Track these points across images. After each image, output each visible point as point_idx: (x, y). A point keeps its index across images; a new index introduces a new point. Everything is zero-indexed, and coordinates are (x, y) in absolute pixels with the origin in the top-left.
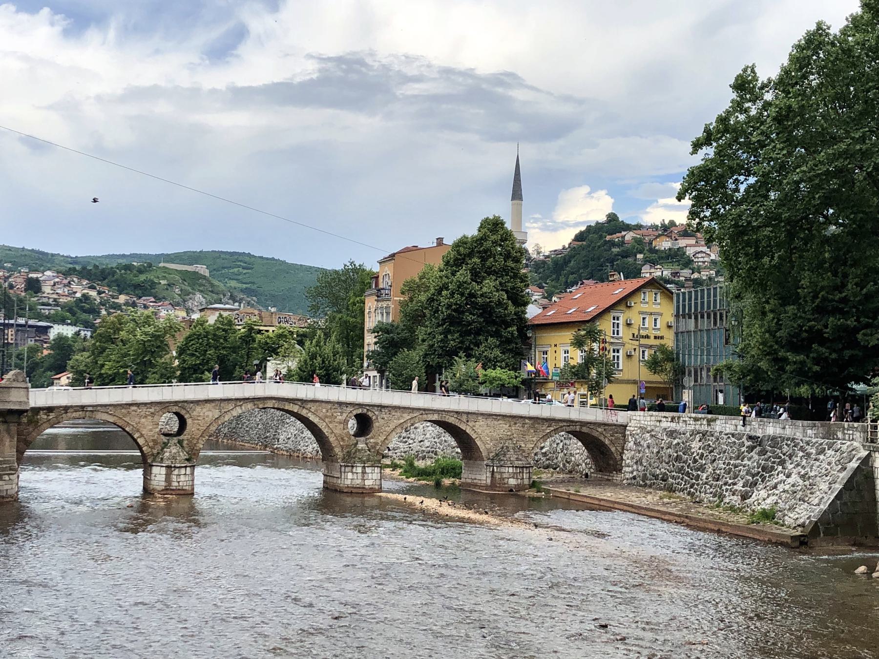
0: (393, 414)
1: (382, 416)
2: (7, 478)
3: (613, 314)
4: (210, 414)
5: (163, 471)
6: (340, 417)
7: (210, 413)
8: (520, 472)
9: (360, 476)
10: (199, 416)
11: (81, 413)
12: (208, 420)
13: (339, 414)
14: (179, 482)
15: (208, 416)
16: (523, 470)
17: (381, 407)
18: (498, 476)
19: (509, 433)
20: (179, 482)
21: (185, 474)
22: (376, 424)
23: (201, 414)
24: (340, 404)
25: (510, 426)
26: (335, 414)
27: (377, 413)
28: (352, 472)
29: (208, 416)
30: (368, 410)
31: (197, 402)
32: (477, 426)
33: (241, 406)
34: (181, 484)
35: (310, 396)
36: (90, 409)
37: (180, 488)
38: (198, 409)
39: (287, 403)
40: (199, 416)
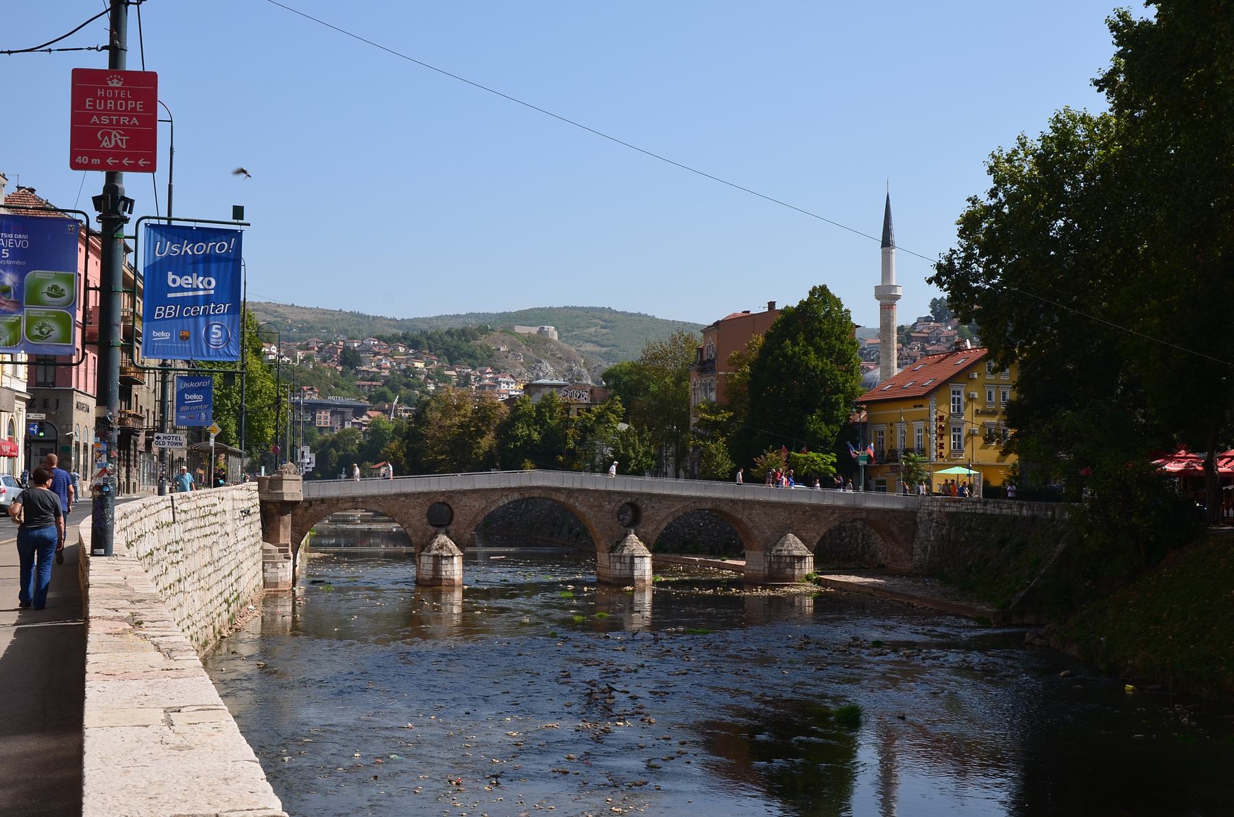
0: (664, 502)
1: (652, 505)
3: (953, 387)
4: (477, 504)
5: (431, 560)
6: (609, 507)
7: (477, 504)
9: (628, 567)
10: (466, 506)
11: (352, 504)
14: (446, 571)
15: (475, 506)
17: (651, 496)
18: (775, 566)
19: (788, 522)
22: (645, 514)
23: (468, 504)
24: (609, 493)
27: (646, 502)
28: (620, 563)
29: (475, 506)
30: (637, 498)
31: (464, 493)
32: (754, 515)
33: (507, 495)
35: (577, 486)
36: (360, 500)
38: (465, 499)
39: (553, 493)
40: (466, 506)
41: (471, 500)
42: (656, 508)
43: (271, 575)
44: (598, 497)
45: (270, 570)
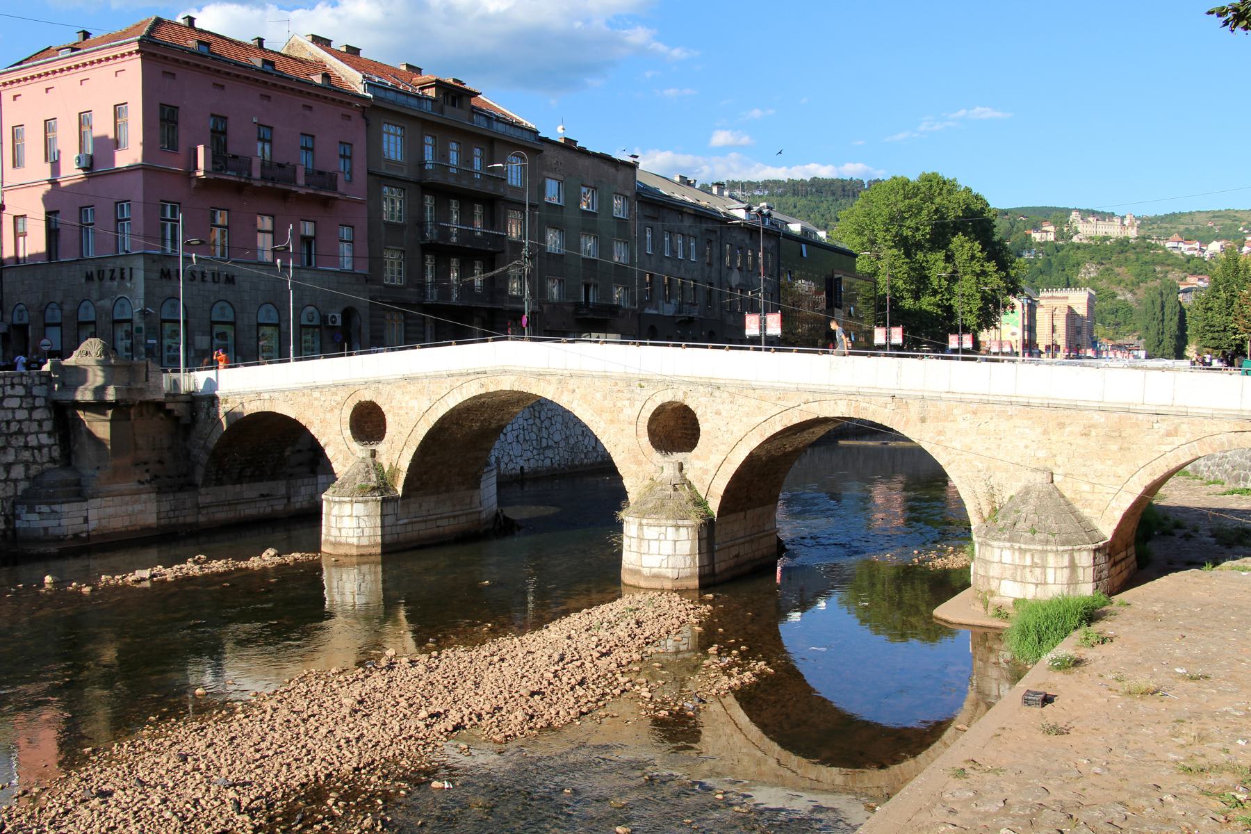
2: (45, 509)
4: (413, 403)
8: (1034, 565)
12: (414, 416)
13: (627, 403)
14: (340, 530)
15: (413, 409)
16: (1044, 560)
17: (714, 387)
19: (1041, 454)
20: (340, 530)
21: (351, 516)
25: (1045, 432)
26: (619, 404)
29: (413, 409)
34: (344, 533)
37: (343, 540)
41: (407, 397)
42: (724, 413)
43: (25, 525)
44: (611, 391)
45: (25, 516)
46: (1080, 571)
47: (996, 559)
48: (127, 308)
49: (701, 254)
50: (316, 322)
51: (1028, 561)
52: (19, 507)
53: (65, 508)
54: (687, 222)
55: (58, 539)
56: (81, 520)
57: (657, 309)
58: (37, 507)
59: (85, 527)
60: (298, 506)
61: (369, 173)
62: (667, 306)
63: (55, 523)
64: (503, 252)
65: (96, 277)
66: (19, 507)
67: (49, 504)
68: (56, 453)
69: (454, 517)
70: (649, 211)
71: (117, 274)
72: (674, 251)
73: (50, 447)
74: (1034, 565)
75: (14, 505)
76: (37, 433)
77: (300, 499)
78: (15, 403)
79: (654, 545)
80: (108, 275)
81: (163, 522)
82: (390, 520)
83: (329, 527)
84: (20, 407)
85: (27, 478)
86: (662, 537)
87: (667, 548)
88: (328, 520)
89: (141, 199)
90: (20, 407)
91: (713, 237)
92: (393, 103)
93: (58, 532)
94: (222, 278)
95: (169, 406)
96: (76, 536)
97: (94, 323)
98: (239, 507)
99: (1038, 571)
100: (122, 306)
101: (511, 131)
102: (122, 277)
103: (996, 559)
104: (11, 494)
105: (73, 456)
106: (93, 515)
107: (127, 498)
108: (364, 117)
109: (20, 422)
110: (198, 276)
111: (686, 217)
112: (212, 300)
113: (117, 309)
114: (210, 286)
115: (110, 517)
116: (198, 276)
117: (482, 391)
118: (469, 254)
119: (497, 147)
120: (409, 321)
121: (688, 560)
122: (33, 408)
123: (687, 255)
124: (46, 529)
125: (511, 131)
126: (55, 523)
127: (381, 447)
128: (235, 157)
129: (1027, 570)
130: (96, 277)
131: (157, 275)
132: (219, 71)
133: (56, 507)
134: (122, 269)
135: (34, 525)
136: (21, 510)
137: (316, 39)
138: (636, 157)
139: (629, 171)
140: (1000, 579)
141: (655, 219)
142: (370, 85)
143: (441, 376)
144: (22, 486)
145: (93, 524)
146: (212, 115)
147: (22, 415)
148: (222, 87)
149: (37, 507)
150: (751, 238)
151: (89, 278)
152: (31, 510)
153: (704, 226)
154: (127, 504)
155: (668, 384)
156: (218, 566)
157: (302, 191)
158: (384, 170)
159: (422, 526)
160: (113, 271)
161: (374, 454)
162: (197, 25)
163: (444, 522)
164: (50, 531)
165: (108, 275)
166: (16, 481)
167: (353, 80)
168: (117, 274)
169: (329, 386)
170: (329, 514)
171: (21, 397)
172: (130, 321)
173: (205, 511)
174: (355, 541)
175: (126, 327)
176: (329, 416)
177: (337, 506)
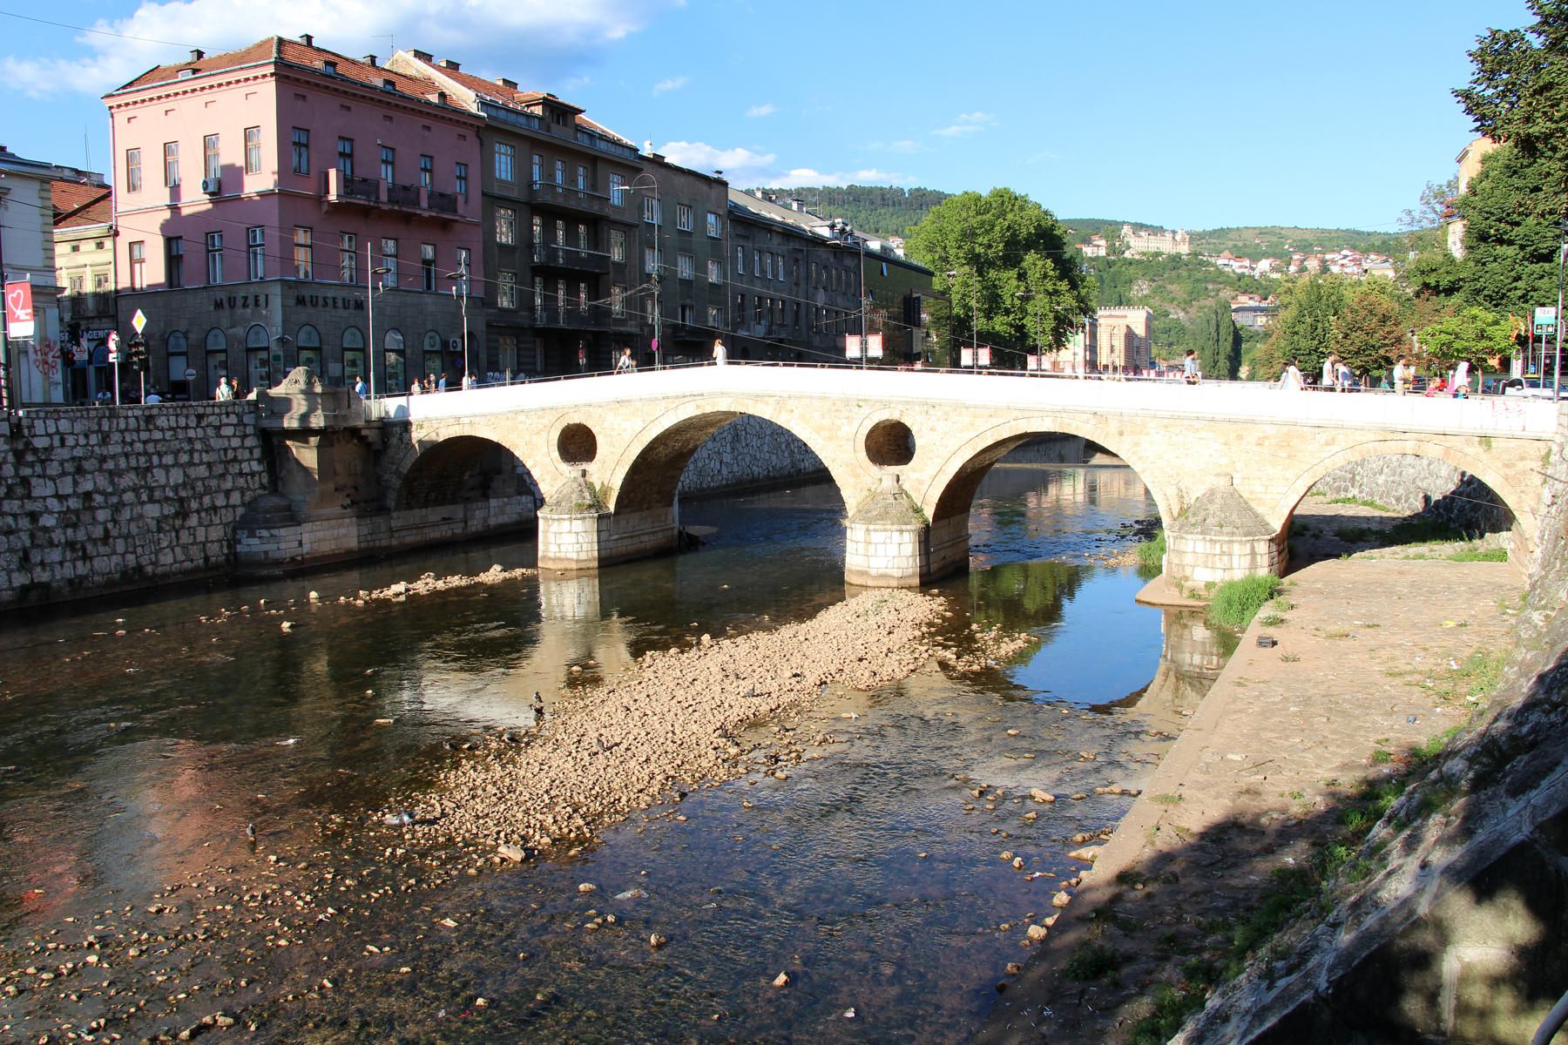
2: (265, 533)
8: (1223, 553)
13: (845, 421)
17: (929, 406)
21: (570, 532)
34: (563, 548)
37: (562, 555)
43: (246, 549)
45: (245, 541)
46: (1259, 557)
47: (1190, 549)
48: (263, 336)
49: (788, 273)
50: (438, 347)
51: (1218, 551)
52: (239, 532)
53: (283, 532)
54: (776, 240)
55: (278, 563)
56: (296, 543)
57: (748, 330)
58: (257, 532)
59: (299, 550)
60: (474, 529)
61: (484, 194)
62: (758, 327)
63: (274, 547)
64: (608, 273)
65: (226, 305)
66: (239, 532)
67: (268, 528)
68: (265, 481)
69: (654, 533)
70: (740, 230)
71: (251, 301)
72: (763, 271)
73: (260, 473)
74: (1223, 553)
75: (234, 530)
76: (249, 460)
77: (475, 522)
78: (228, 431)
79: (881, 548)
80: (240, 302)
81: (363, 545)
82: (604, 535)
83: (547, 544)
84: (234, 436)
85: (243, 504)
86: (888, 540)
87: (893, 550)
88: (546, 537)
89: (277, 224)
90: (234, 436)
91: (800, 256)
92: (505, 122)
93: (277, 555)
94: (352, 303)
95: (364, 432)
96: (293, 559)
97: (225, 351)
98: (425, 531)
99: (1225, 558)
100: (257, 333)
101: (612, 149)
102: (257, 304)
103: (1190, 549)
104: (231, 519)
105: (280, 483)
106: (306, 538)
107: (334, 522)
108: (478, 137)
109: (235, 449)
110: (330, 302)
111: (774, 235)
112: (343, 326)
113: (252, 336)
114: (341, 312)
115: (320, 540)
116: (330, 302)
117: (699, 412)
118: (573, 276)
119: (600, 166)
120: (522, 346)
121: (911, 560)
122: (244, 437)
123: (775, 275)
124: (266, 553)
125: (612, 149)
126: (274, 547)
127: (591, 467)
128: (365, 180)
129: (1217, 558)
130: (226, 305)
131: (292, 302)
132: (346, 92)
133: (275, 532)
134: (256, 297)
135: (254, 549)
136: (242, 535)
137: (419, 54)
138: (720, 173)
139: (721, 188)
140: (1194, 567)
141: (746, 238)
142: (484, 104)
143: (656, 399)
144: (240, 511)
145: (306, 548)
146: (340, 138)
147: (236, 442)
148: (349, 108)
149: (257, 532)
150: (835, 257)
151: (219, 305)
152: (252, 535)
153: (791, 246)
154: (333, 528)
155: (886, 405)
156: (456, 581)
157: (426, 214)
158: (497, 191)
159: (628, 542)
160: (246, 298)
161: (584, 473)
162: (315, 43)
163: (645, 538)
164: (270, 555)
165: (240, 302)
166: (234, 507)
167: (467, 99)
168: (251, 301)
169: (536, 410)
170: (546, 532)
171: (234, 425)
172: (267, 349)
173: (396, 535)
174: (574, 556)
175: (264, 355)
176: (535, 438)
177: (556, 523)
